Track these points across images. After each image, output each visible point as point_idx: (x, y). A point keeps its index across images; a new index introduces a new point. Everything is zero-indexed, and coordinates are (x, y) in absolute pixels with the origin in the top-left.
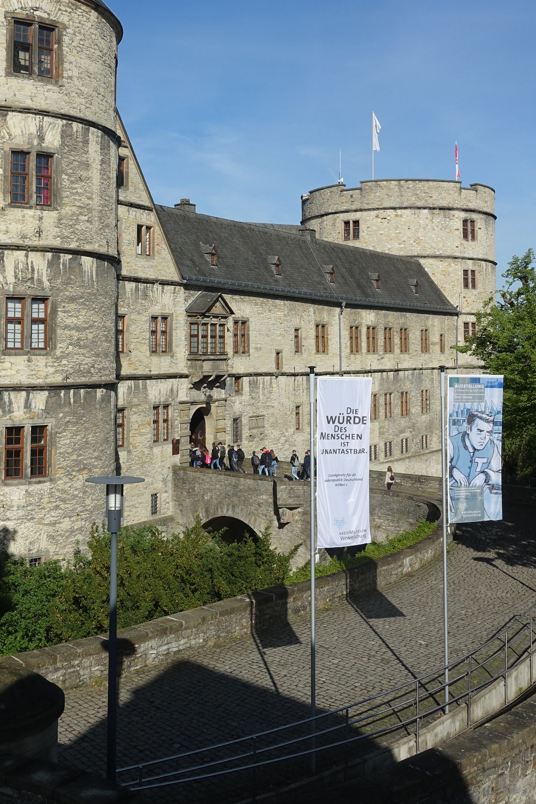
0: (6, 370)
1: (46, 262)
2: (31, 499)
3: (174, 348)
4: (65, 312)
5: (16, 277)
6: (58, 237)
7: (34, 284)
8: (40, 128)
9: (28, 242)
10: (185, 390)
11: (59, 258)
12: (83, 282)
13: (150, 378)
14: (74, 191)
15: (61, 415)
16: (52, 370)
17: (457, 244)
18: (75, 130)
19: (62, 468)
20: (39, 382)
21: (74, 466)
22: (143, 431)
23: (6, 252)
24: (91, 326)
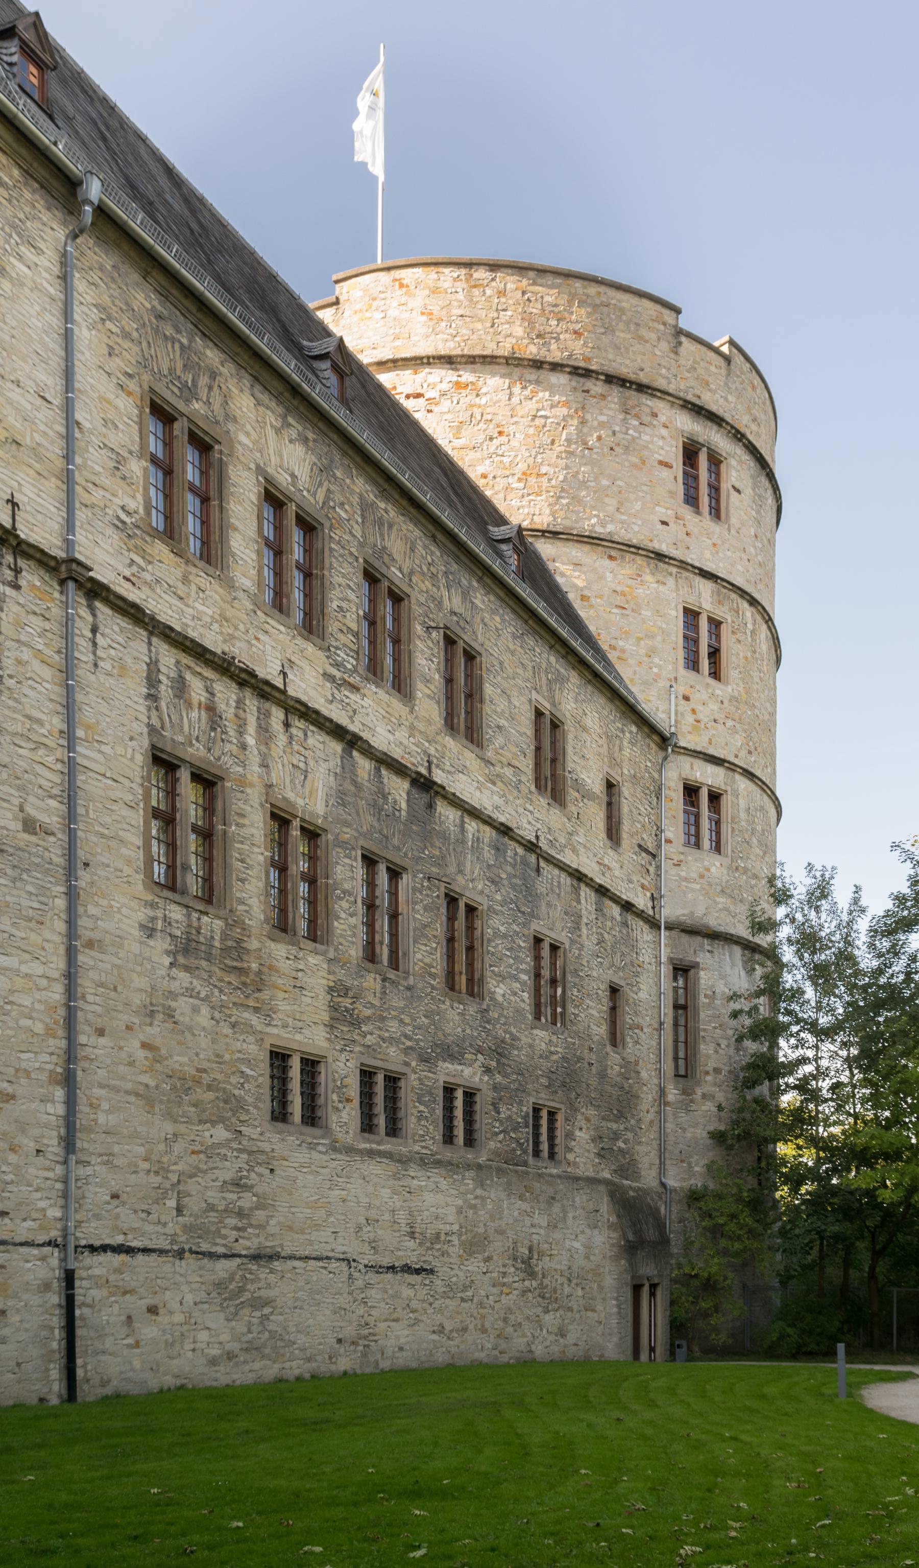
17: (661, 512)
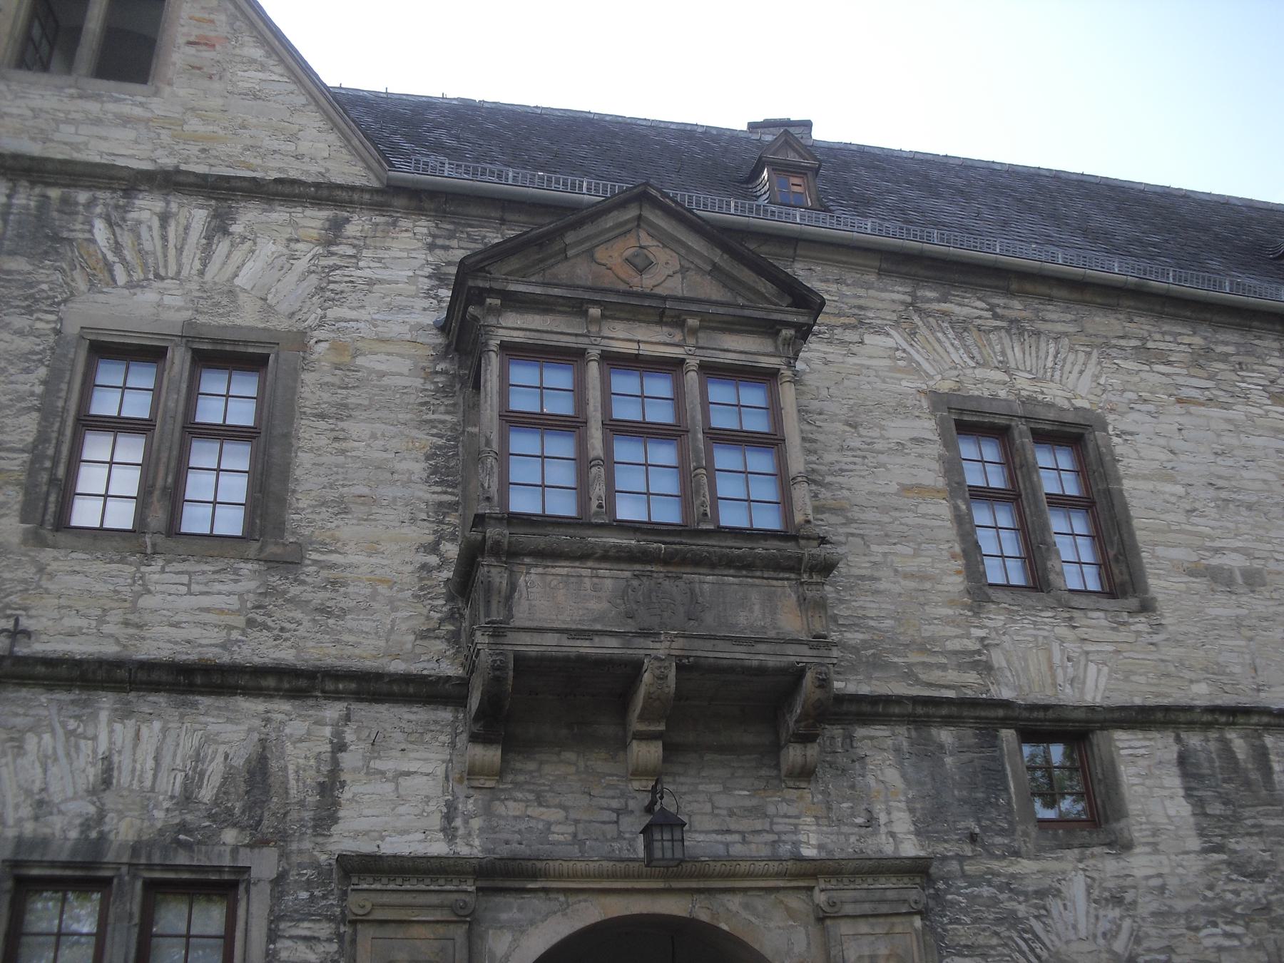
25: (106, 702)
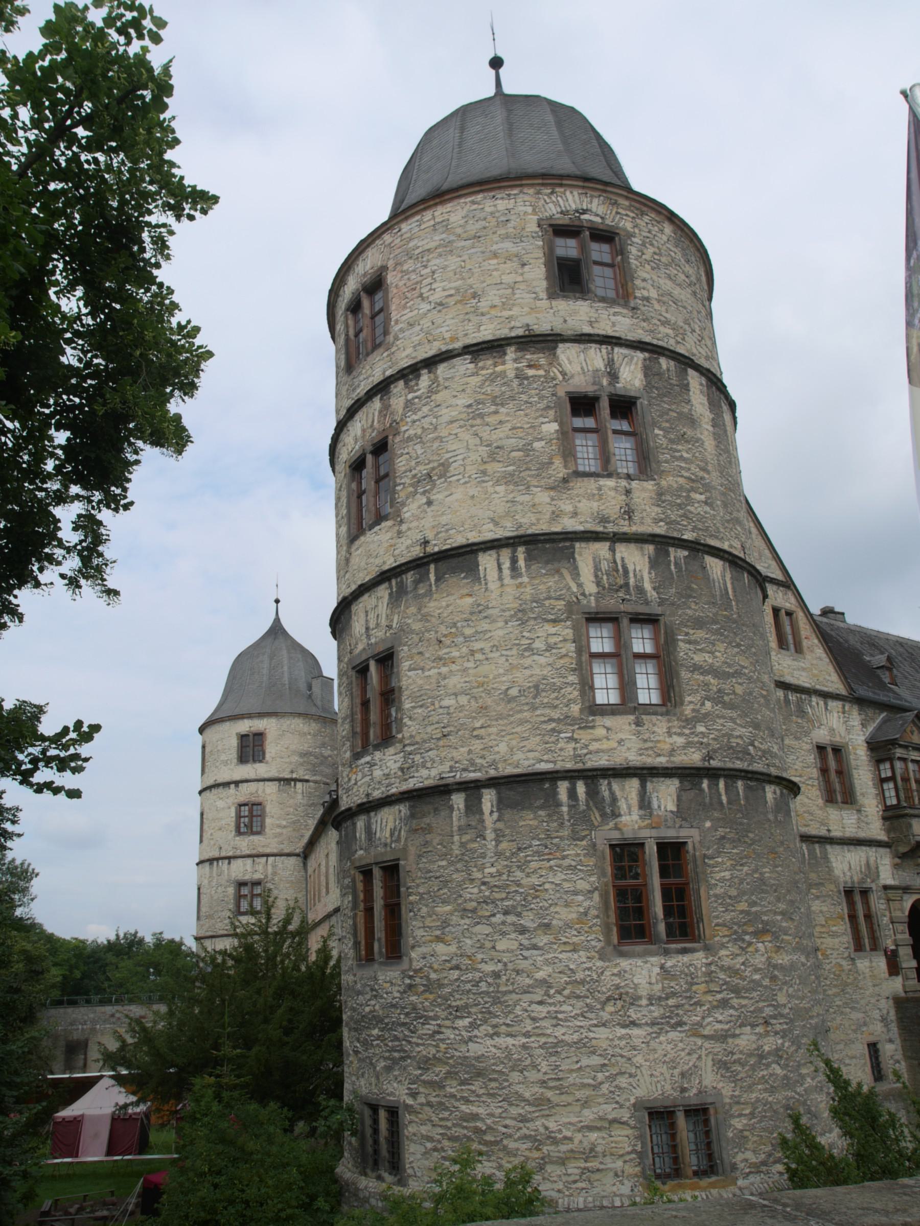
0: (599, 740)
1: (647, 560)
2: (672, 984)
3: (859, 798)
4: (690, 642)
5: (598, 583)
6: (661, 520)
7: (630, 595)
8: (610, 363)
9: (611, 528)
10: (888, 867)
11: (668, 554)
12: (714, 596)
13: (832, 841)
14: (677, 454)
15: (708, 824)
16: (680, 741)
18: (664, 367)
19: (724, 925)
20: (662, 761)
21: (745, 924)
22: (834, 929)
23: (577, 545)
24: (737, 674)
25: (846, 847)
